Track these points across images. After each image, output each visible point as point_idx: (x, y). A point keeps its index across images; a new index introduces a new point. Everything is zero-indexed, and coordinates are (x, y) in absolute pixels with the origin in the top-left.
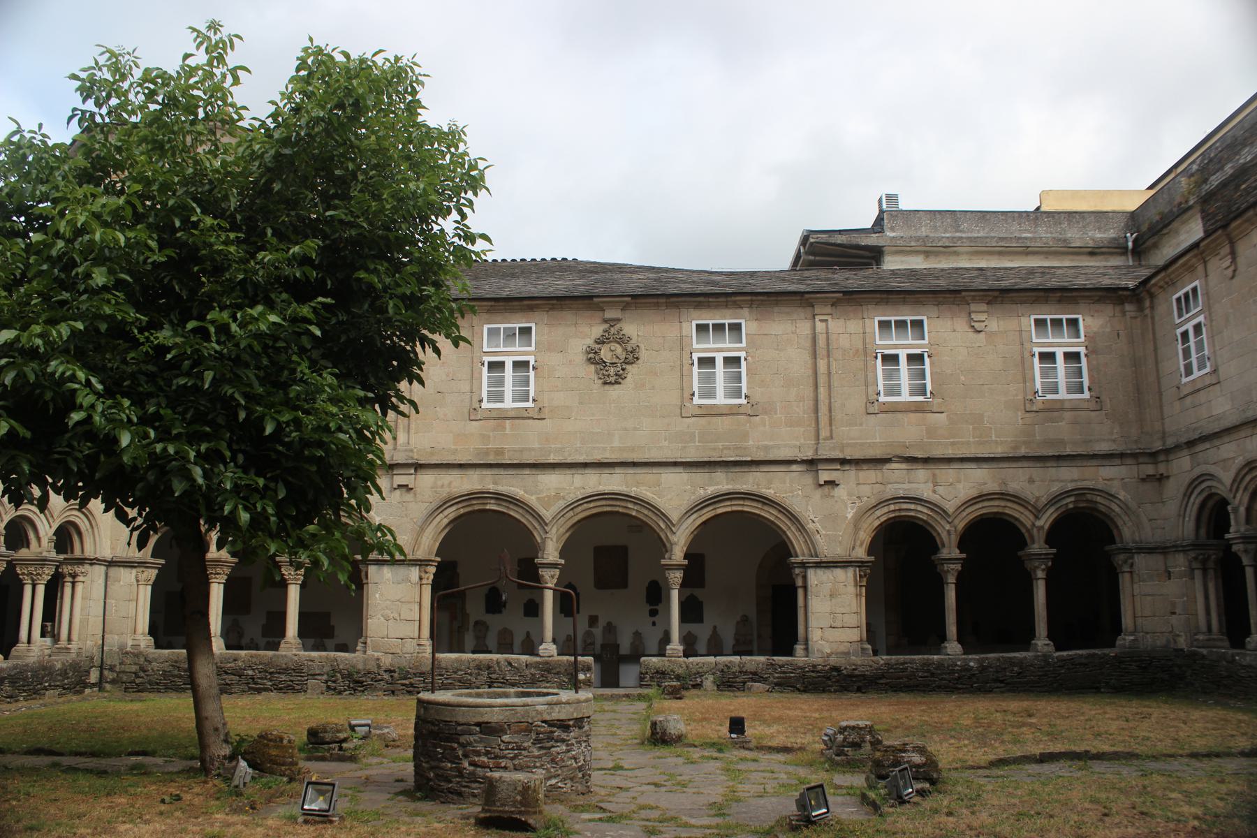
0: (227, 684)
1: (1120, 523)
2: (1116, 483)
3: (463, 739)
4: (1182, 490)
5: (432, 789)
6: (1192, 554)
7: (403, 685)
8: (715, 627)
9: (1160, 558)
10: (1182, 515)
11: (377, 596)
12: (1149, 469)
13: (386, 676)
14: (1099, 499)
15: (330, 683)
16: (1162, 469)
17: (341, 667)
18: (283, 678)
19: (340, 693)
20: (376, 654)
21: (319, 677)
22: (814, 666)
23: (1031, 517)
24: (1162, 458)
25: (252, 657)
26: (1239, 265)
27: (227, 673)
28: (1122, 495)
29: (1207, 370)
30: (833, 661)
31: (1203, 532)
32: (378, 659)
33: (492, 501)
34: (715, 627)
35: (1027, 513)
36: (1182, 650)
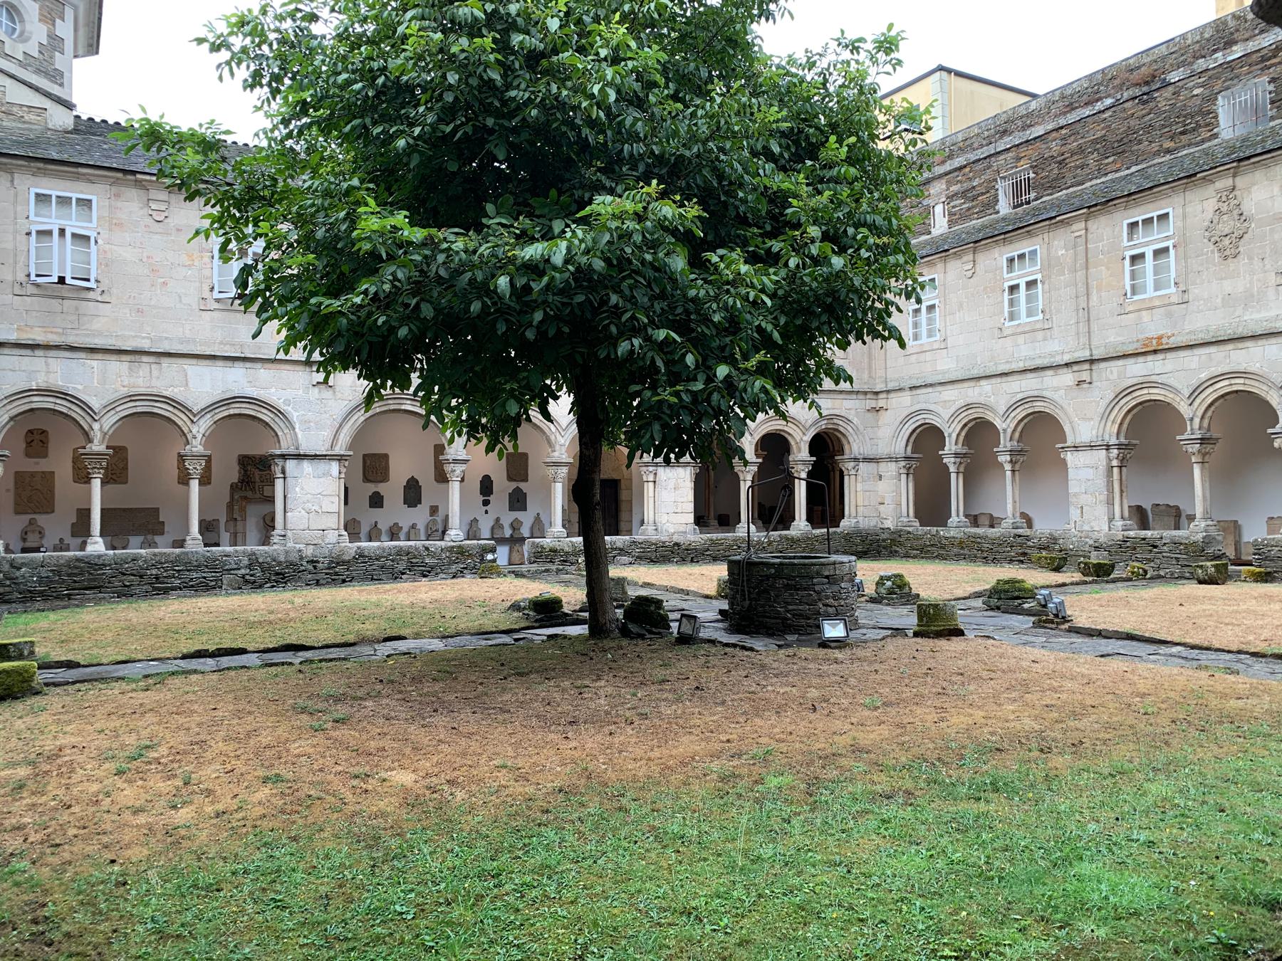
0: (126, 586)
1: (851, 439)
2: (853, 412)
3: (817, 588)
4: (900, 419)
5: (790, 626)
6: (903, 463)
7: (327, 574)
8: (538, 514)
9: (875, 465)
10: (896, 436)
11: (297, 489)
12: (873, 404)
13: (310, 567)
14: (841, 423)
15: (247, 577)
16: (881, 403)
17: (260, 560)
18: (195, 575)
19: (261, 587)
20: (298, 546)
21: (235, 572)
22: (664, 542)
23: (801, 433)
24: (882, 396)
25: (155, 555)
26: (978, 269)
27: (124, 574)
28: (855, 420)
29: (938, 338)
30: (676, 538)
31: (909, 448)
32: (300, 551)
33: (409, 402)
34: (538, 514)
35: (798, 430)
36: (889, 529)
